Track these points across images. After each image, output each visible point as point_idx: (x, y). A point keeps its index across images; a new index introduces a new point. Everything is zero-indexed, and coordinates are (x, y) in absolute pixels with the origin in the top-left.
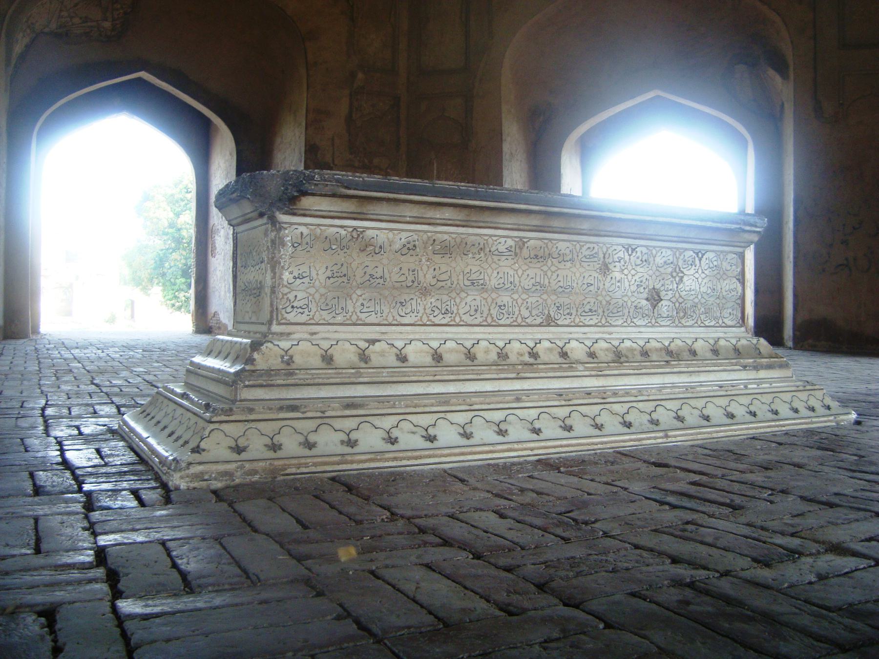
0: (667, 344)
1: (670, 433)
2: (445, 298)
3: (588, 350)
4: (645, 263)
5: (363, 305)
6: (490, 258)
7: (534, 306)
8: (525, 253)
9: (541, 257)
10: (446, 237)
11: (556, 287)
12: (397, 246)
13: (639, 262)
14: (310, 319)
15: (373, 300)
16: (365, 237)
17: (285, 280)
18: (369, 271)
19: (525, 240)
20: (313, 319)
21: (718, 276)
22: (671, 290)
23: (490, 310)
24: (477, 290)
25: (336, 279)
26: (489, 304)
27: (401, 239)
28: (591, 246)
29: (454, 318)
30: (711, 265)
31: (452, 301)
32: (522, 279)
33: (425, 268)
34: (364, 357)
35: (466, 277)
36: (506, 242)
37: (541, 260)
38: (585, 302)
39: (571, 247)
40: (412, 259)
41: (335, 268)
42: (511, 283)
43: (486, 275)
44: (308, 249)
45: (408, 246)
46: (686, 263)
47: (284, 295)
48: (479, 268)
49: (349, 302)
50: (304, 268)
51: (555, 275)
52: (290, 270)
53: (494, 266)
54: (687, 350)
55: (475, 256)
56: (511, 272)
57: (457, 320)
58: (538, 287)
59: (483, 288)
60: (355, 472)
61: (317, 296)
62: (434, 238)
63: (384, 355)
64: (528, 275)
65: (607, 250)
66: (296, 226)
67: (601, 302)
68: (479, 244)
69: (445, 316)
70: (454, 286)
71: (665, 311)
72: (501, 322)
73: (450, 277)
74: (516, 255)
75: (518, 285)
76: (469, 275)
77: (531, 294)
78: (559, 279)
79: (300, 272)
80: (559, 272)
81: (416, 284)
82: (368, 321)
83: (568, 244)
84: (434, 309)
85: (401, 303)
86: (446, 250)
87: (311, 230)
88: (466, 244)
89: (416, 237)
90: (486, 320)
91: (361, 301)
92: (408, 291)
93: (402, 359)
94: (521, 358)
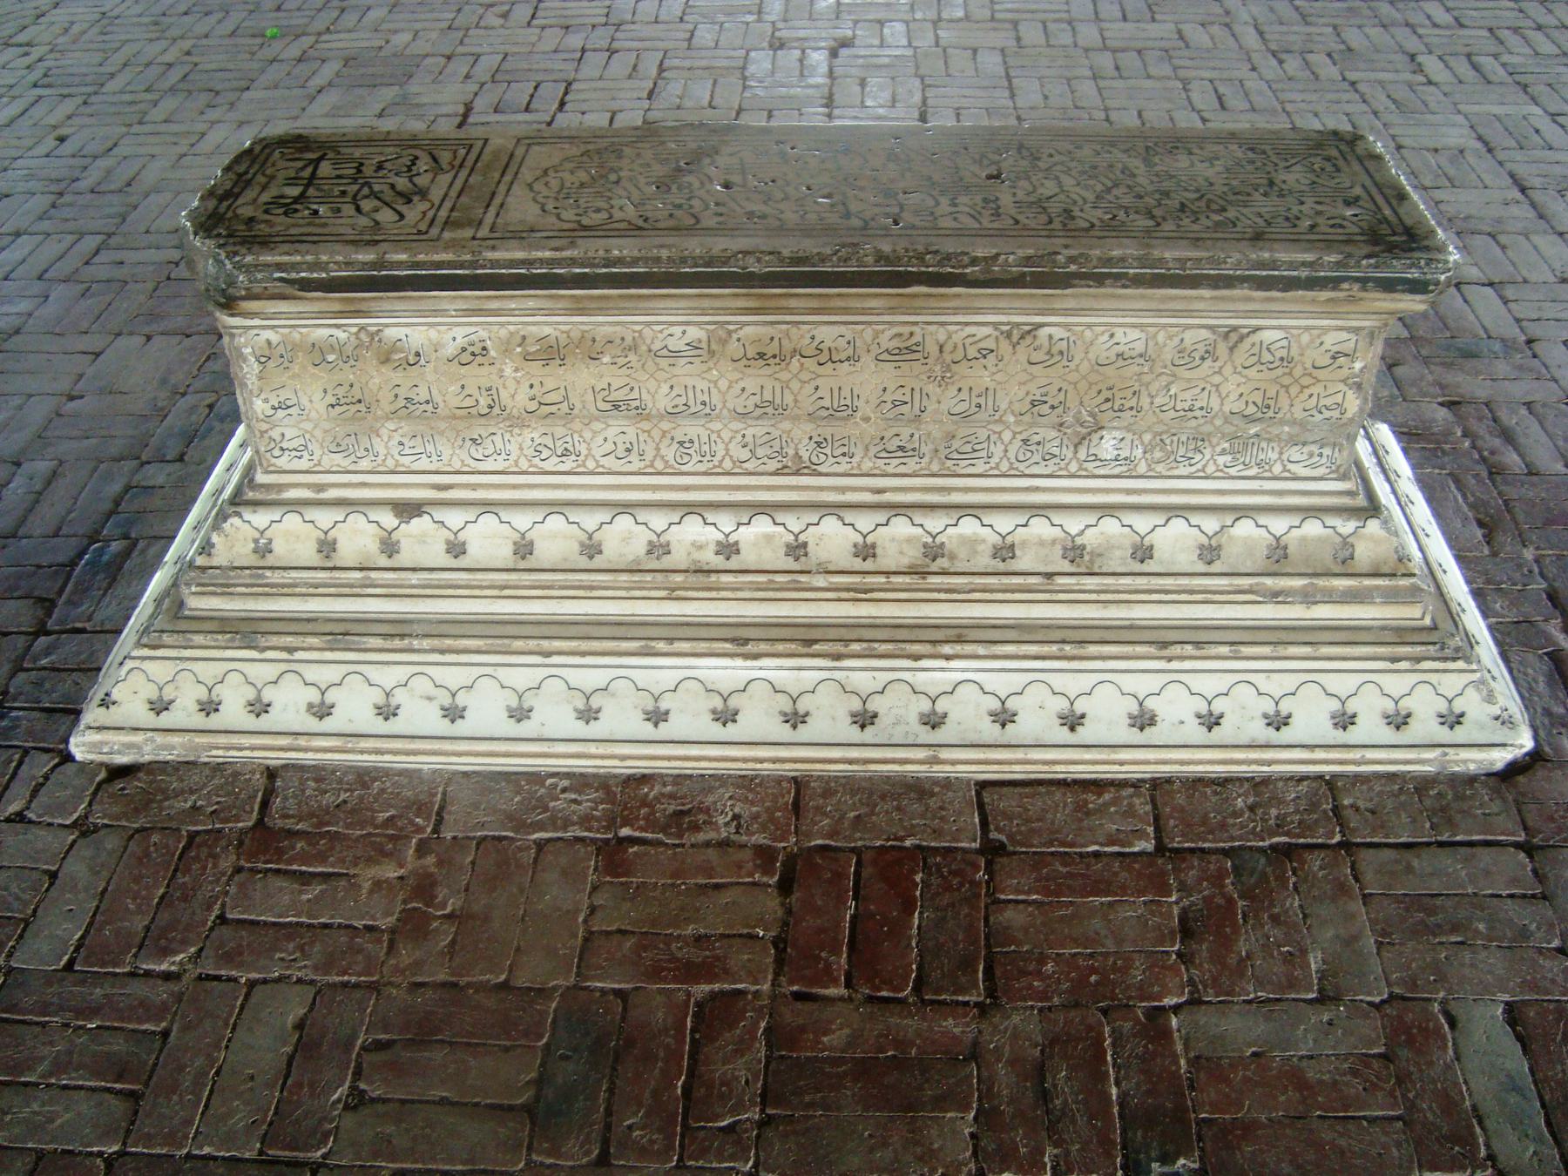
0: (1074, 532)
1: (945, 754)
2: (560, 431)
3: (860, 539)
4: (1057, 358)
5: (401, 444)
6: (650, 363)
7: (759, 442)
8: (734, 348)
9: (774, 356)
10: (547, 330)
11: (811, 410)
12: (451, 350)
13: (1039, 356)
14: (315, 465)
15: (419, 438)
16: (384, 340)
17: (259, 411)
18: (402, 392)
19: (731, 327)
20: (319, 464)
21: (1286, 381)
22: (1132, 408)
23: (658, 449)
24: (628, 417)
25: (345, 408)
26: (657, 440)
27: (454, 339)
28: (906, 330)
29: (584, 461)
30: (1267, 357)
31: (576, 436)
32: (728, 397)
33: (511, 385)
34: (389, 546)
35: (600, 397)
36: (684, 332)
37: (772, 361)
38: (888, 435)
39: (849, 337)
40: (485, 370)
41: (341, 392)
42: (703, 403)
43: (643, 391)
44: (285, 365)
45: (471, 349)
46: (1186, 355)
47: (262, 433)
48: (627, 380)
49: (376, 440)
50: (284, 394)
51: (809, 389)
52: (263, 396)
53: (661, 375)
54: (1127, 543)
55: (616, 360)
56: (702, 385)
57: (591, 465)
58: (770, 410)
59: (641, 413)
60: (314, 763)
61: (318, 433)
62: (522, 333)
63: (424, 542)
64: (743, 390)
65: (950, 337)
66: (256, 332)
67: (929, 434)
68: (623, 339)
69: (564, 459)
70: (576, 411)
71: (1110, 449)
72: (684, 468)
73: (566, 398)
74: (712, 353)
75: (719, 406)
76: (606, 393)
77: (750, 422)
78: (819, 394)
79: (282, 400)
80: (819, 382)
81: (496, 410)
82: (415, 467)
83: (842, 329)
84: (539, 448)
85: (474, 440)
86: (551, 353)
87: (282, 335)
88: (594, 340)
89: (483, 334)
90: (652, 466)
91: (397, 438)
92: (483, 421)
93: (456, 549)
94: (697, 555)
